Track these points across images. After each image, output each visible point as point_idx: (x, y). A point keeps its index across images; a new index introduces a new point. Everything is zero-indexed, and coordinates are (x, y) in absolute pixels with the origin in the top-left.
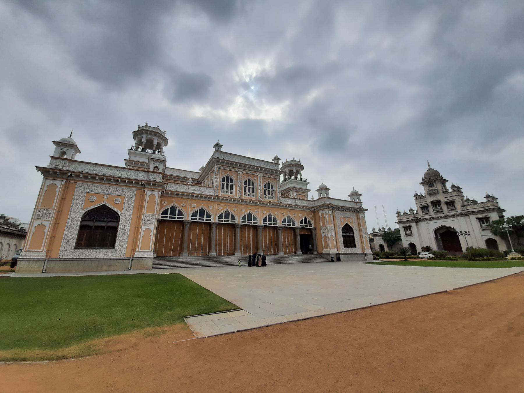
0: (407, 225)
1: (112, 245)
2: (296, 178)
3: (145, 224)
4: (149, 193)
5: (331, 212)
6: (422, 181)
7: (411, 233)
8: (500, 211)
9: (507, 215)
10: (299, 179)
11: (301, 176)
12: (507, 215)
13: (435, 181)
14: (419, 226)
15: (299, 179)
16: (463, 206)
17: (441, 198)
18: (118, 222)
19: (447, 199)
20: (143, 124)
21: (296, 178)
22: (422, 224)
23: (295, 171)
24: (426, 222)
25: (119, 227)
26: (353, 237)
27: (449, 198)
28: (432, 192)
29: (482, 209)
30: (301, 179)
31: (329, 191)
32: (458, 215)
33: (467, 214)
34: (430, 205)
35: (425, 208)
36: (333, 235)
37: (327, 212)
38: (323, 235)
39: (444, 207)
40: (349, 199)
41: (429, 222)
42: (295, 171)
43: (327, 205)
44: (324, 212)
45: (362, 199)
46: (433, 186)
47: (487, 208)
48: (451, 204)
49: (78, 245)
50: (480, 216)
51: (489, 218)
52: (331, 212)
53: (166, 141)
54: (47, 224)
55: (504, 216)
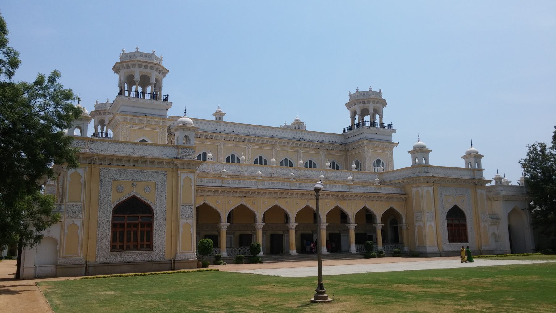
1: (150, 247)
2: (373, 124)
3: (183, 217)
4: (183, 176)
5: (430, 189)
10: (377, 125)
11: (381, 117)
15: (377, 125)
18: (152, 217)
20: (130, 49)
21: (373, 124)
23: (371, 111)
25: (155, 224)
26: (465, 226)
30: (382, 125)
31: (430, 154)
36: (433, 224)
37: (426, 189)
38: (416, 225)
40: (462, 164)
42: (371, 111)
43: (422, 170)
44: (419, 189)
45: (484, 163)
49: (113, 248)
52: (430, 189)
53: (164, 72)
54: (78, 223)
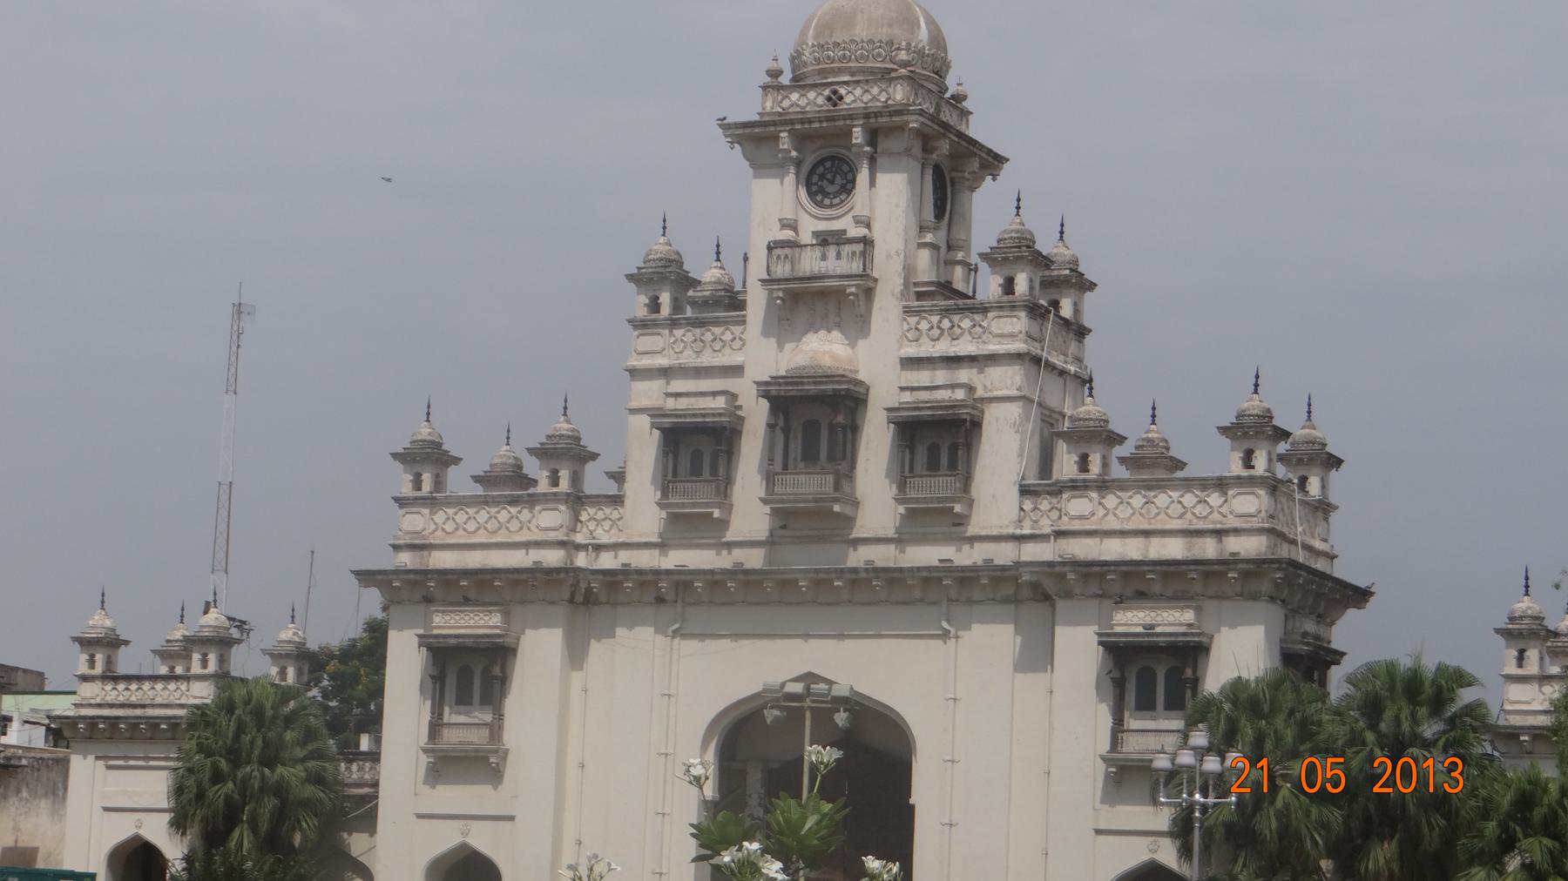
8: (1310, 594)
9: (1360, 641)
12: (1360, 641)
13: (873, 136)
16: (1039, 486)
19: (922, 377)
27: (941, 376)
28: (810, 263)
33: (1033, 594)
34: (757, 414)
46: (848, 187)
48: (939, 440)
50: (1171, 620)
55: (1337, 657)
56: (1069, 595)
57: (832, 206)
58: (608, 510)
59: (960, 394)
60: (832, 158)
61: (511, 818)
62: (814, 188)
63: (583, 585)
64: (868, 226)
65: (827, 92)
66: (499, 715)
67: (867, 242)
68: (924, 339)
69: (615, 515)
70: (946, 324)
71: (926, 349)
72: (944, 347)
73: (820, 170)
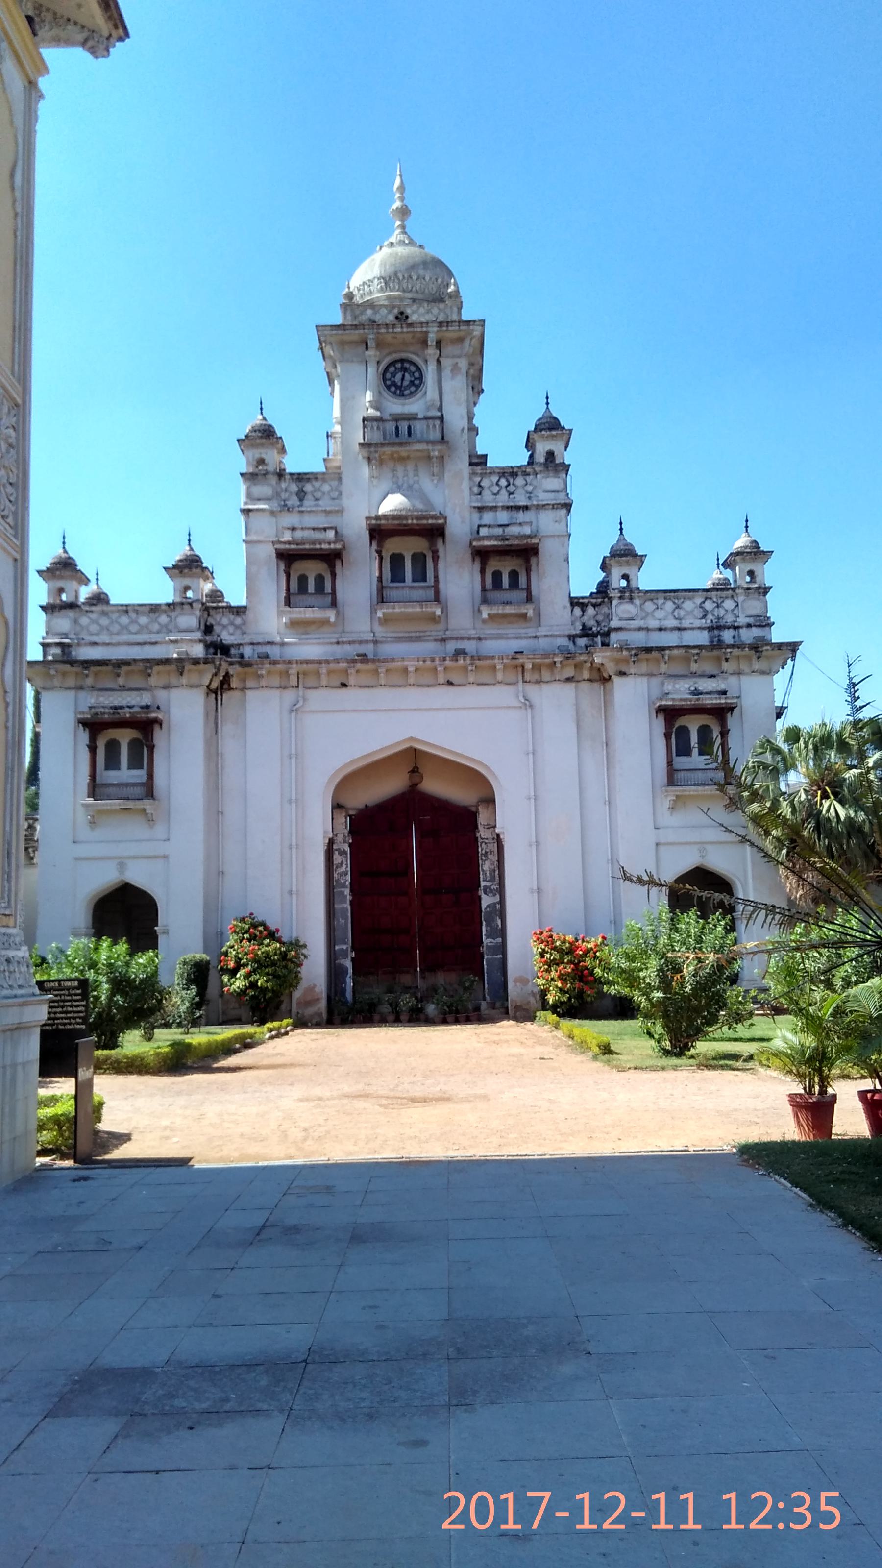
0: (131, 700)
6: (337, 318)
7: (149, 790)
14: (227, 729)
17: (453, 500)
22: (262, 709)
24: (289, 696)
27: (503, 517)
29: (703, 638)
32: (525, 669)
35: (308, 568)
39: (459, 580)
41: (318, 698)
46: (418, 382)
47: (727, 636)
51: (731, 709)
56: (622, 674)
57: (403, 395)
58: (232, 617)
59: (527, 530)
60: (402, 361)
61: (165, 857)
62: (388, 383)
63: (222, 673)
64: (440, 409)
65: (396, 311)
66: (150, 775)
67: (442, 419)
68: (487, 494)
69: (238, 621)
70: (503, 482)
71: (488, 499)
72: (503, 499)
73: (392, 369)
